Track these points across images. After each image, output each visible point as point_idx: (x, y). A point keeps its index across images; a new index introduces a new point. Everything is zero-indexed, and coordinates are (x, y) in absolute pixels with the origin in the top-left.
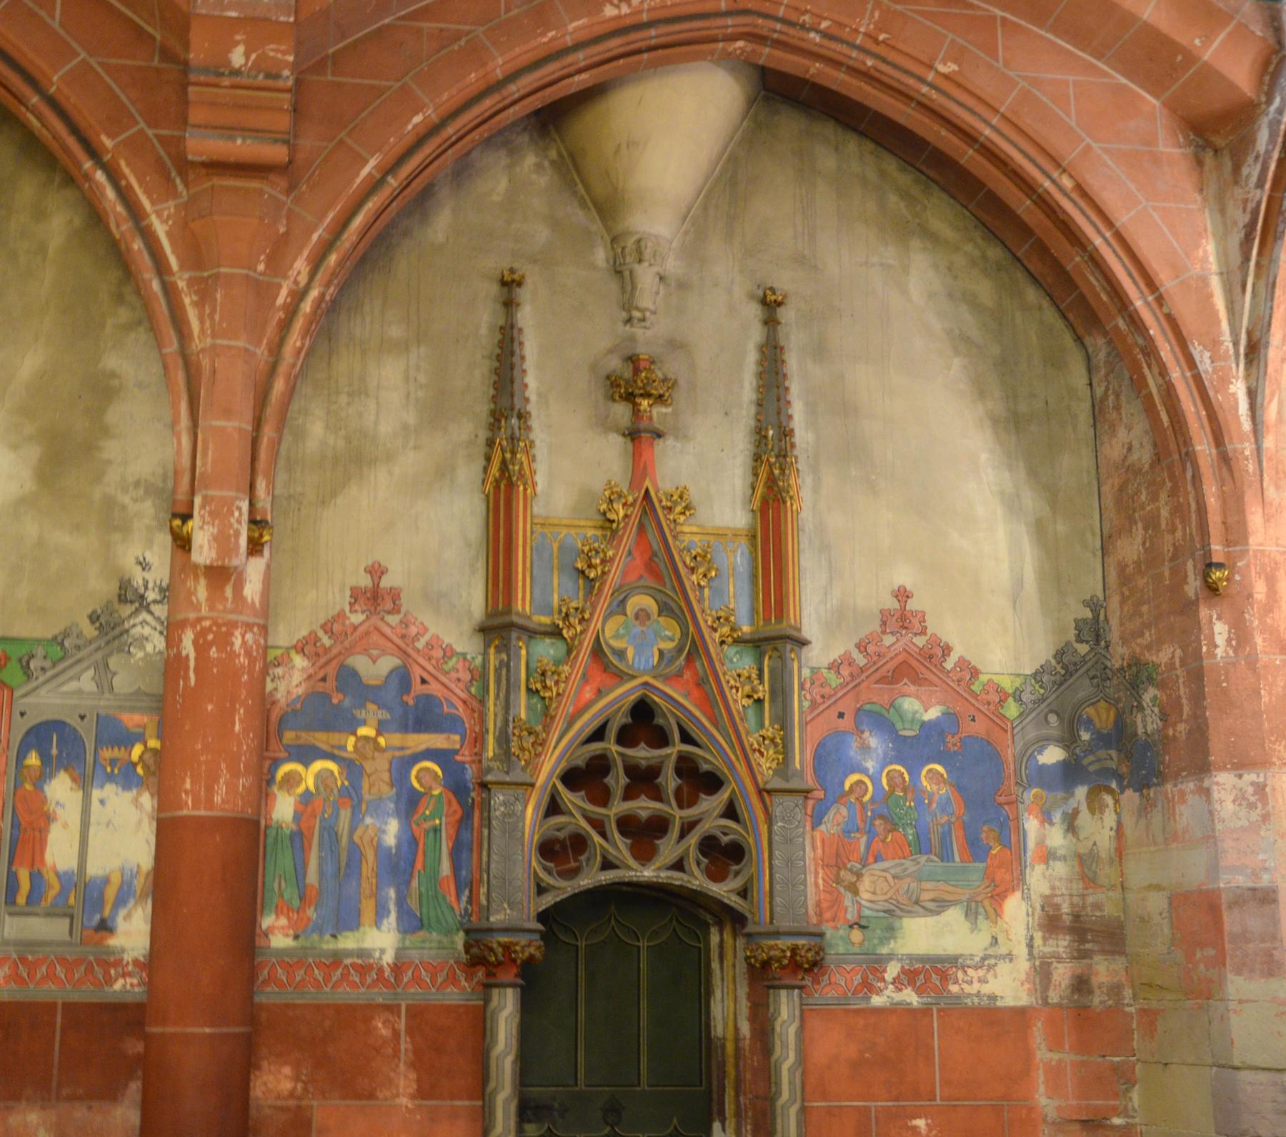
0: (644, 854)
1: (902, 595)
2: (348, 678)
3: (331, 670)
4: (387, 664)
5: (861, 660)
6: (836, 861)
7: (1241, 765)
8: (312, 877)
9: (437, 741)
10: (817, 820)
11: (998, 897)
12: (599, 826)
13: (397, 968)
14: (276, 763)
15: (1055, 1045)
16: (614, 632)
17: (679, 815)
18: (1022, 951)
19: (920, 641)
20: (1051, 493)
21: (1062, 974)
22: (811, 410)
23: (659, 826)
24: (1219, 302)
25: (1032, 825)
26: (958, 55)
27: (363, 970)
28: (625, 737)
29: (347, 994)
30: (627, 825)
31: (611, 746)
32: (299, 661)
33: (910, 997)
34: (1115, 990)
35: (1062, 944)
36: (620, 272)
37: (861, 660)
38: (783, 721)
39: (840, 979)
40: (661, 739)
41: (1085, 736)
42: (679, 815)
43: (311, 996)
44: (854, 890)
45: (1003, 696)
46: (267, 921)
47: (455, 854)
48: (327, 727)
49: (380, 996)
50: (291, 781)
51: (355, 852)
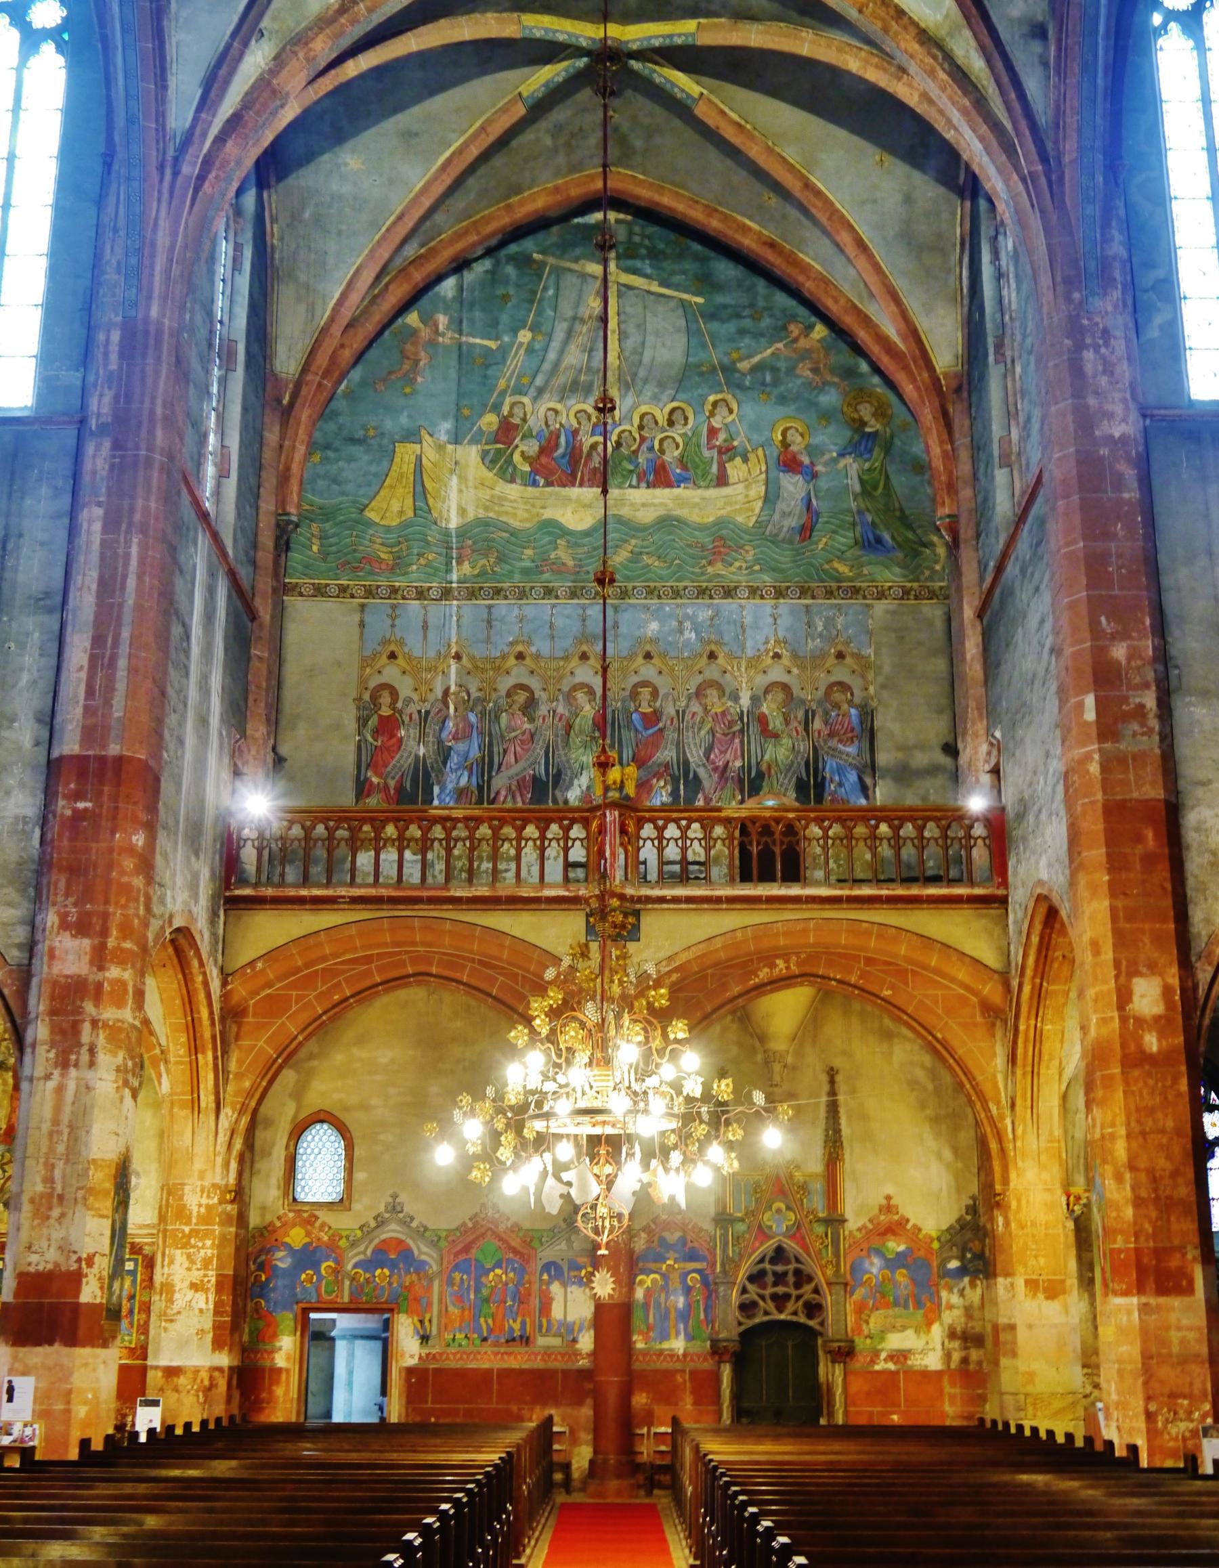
0: (781, 1311)
1: (888, 1198)
2: (662, 1241)
3: (656, 1238)
4: (677, 1235)
5: (870, 1226)
6: (860, 1309)
7: (1007, 1274)
8: (651, 1320)
9: (698, 1265)
10: (852, 1294)
11: (929, 1324)
12: (763, 1298)
13: (685, 1355)
14: (636, 1276)
15: (953, 1384)
16: (767, 1219)
17: (794, 1293)
18: (939, 1347)
19: (896, 1217)
20: (956, 1151)
21: (956, 1357)
22: (849, 1118)
23: (787, 1297)
24: (1001, 1085)
25: (944, 1294)
26: (892, 987)
27: (672, 1356)
28: (773, 1261)
29: (666, 1366)
30: (774, 1297)
31: (767, 1266)
32: (643, 1235)
33: (891, 1366)
34: (980, 1363)
35: (956, 1344)
36: (767, 1063)
37: (870, 1226)
38: (837, 1254)
39: (861, 1359)
40: (788, 1262)
41: (969, 1255)
42: (794, 1293)
43: (652, 1366)
44: (867, 1322)
45: (932, 1240)
46: (635, 1338)
47: (705, 1310)
48: (656, 1261)
49: (678, 1366)
50: (642, 1282)
51: (667, 1310)
